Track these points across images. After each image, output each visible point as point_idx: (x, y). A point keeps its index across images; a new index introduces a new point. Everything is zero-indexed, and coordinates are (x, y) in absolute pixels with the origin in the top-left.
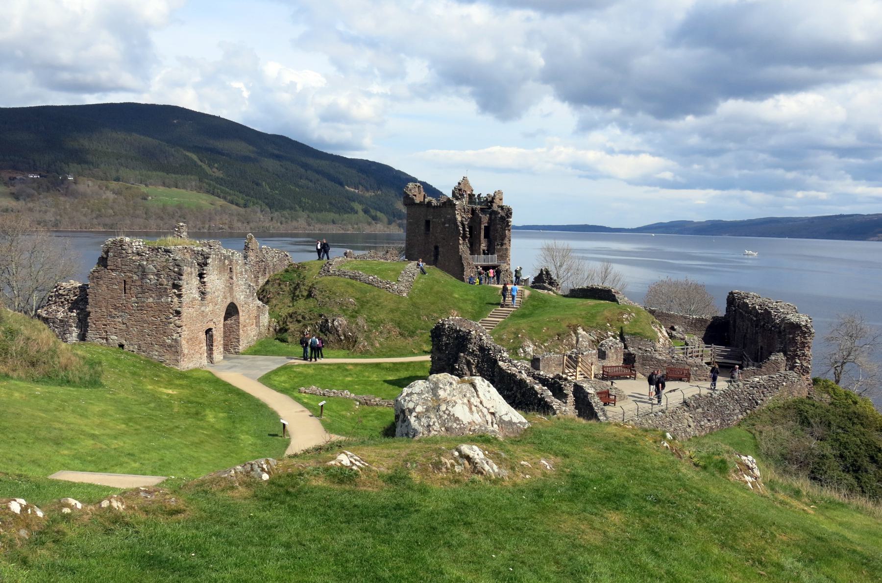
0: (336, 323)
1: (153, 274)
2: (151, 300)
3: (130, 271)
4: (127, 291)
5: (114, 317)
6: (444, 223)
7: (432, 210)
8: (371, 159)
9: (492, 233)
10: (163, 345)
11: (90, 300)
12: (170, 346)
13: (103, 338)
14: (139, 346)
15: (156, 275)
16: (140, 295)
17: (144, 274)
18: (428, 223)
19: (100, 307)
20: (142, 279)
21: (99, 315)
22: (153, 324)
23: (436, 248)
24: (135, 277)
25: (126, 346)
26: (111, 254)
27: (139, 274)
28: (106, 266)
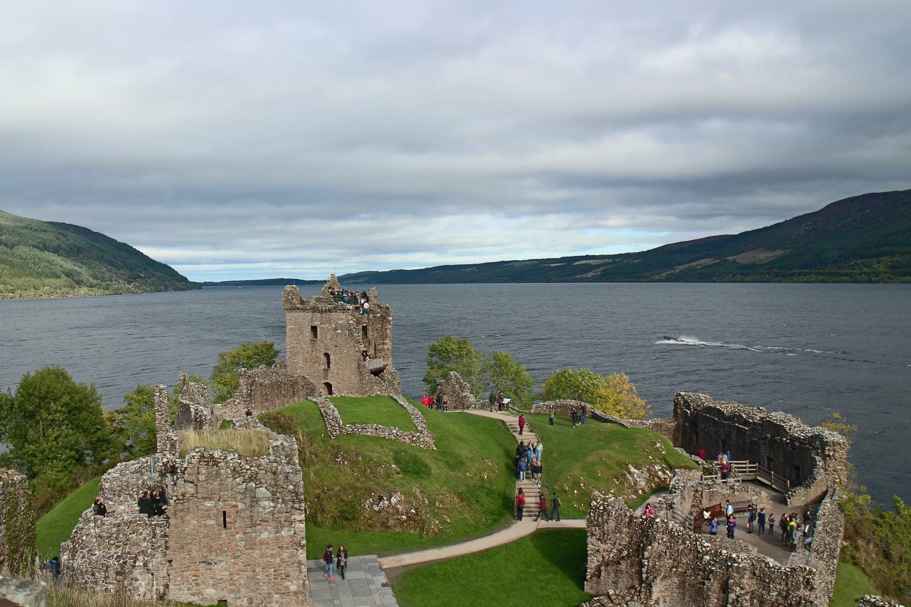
0: (393, 500)
1: (268, 499)
2: (265, 535)
5: (210, 564)
6: (336, 329)
7: (319, 315)
10: (286, 593)
12: (296, 593)
13: (193, 595)
15: (273, 501)
16: (249, 530)
18: (314, 329)
21: (187, 562)
23: (327, 355)
24: (241, 506)
27: (248, 501)
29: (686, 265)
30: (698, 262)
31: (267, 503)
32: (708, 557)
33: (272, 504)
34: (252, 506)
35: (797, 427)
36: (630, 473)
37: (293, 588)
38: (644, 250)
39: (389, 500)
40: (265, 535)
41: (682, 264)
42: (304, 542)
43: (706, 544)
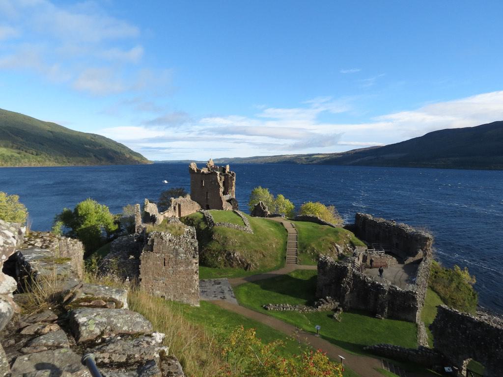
0: (235, 255)
1: (183, 253)
2: (182, 269)
3: (169, 253)
4: (166, 264)
6: (212, 182)
8: (107, 136)
9: (226, 184)
11: (141, 272)
12: (193, 294)
14: (175, 296)
15: (185, 254)
17: (177, 254)
19: (148, 275)
20: (176, 256)
22: (183, 282)
24: (172, 256)
25: (166, 297)
26: (155, 243)
27: (174, 254)
28: (152, 250)
29: (361, 159)
30: (367, 157)
31: (182, 255)
32: (370, 284)
33: (185, 255)
34: (176, 256)
35: (410, 229)
36: (336, 247)
37: (193, 291)
38: (408, 139)
39: (234, 254)
40: (182, 269)
41: (360, 158)
42: (198, 272)
43: (369, 279)
